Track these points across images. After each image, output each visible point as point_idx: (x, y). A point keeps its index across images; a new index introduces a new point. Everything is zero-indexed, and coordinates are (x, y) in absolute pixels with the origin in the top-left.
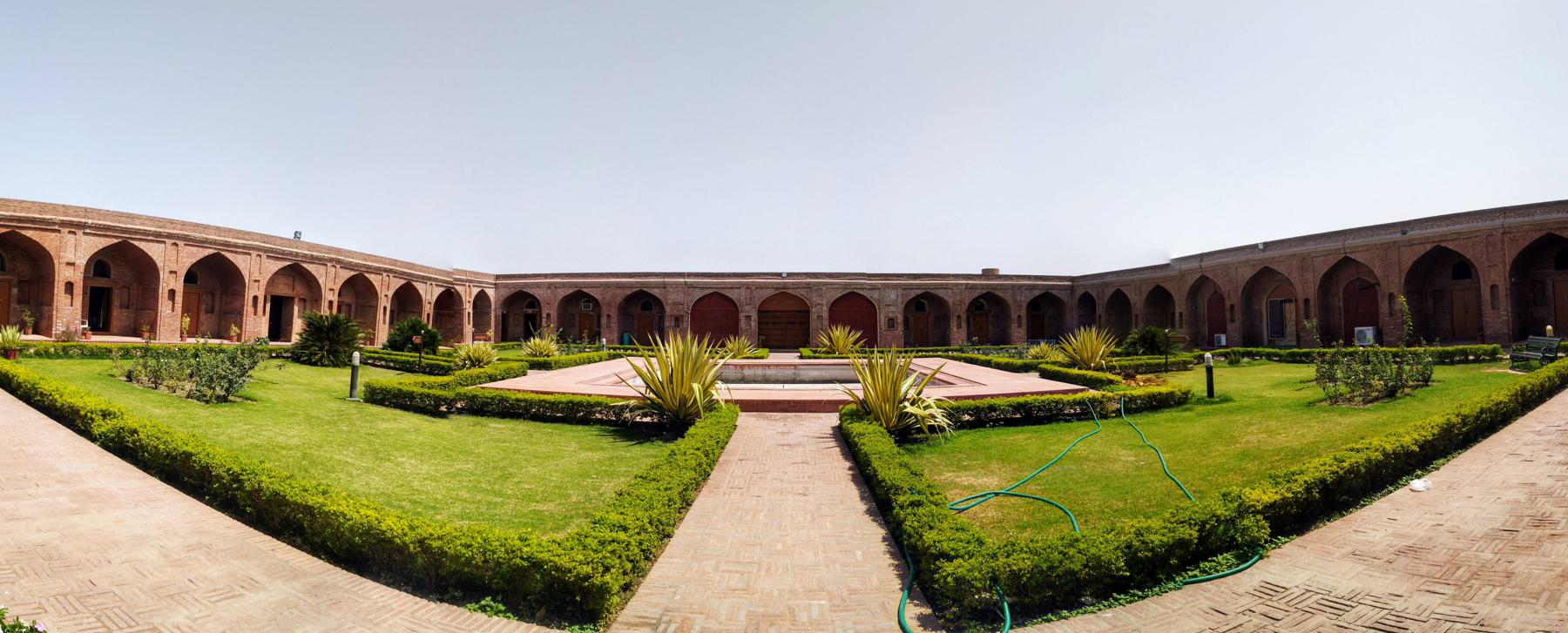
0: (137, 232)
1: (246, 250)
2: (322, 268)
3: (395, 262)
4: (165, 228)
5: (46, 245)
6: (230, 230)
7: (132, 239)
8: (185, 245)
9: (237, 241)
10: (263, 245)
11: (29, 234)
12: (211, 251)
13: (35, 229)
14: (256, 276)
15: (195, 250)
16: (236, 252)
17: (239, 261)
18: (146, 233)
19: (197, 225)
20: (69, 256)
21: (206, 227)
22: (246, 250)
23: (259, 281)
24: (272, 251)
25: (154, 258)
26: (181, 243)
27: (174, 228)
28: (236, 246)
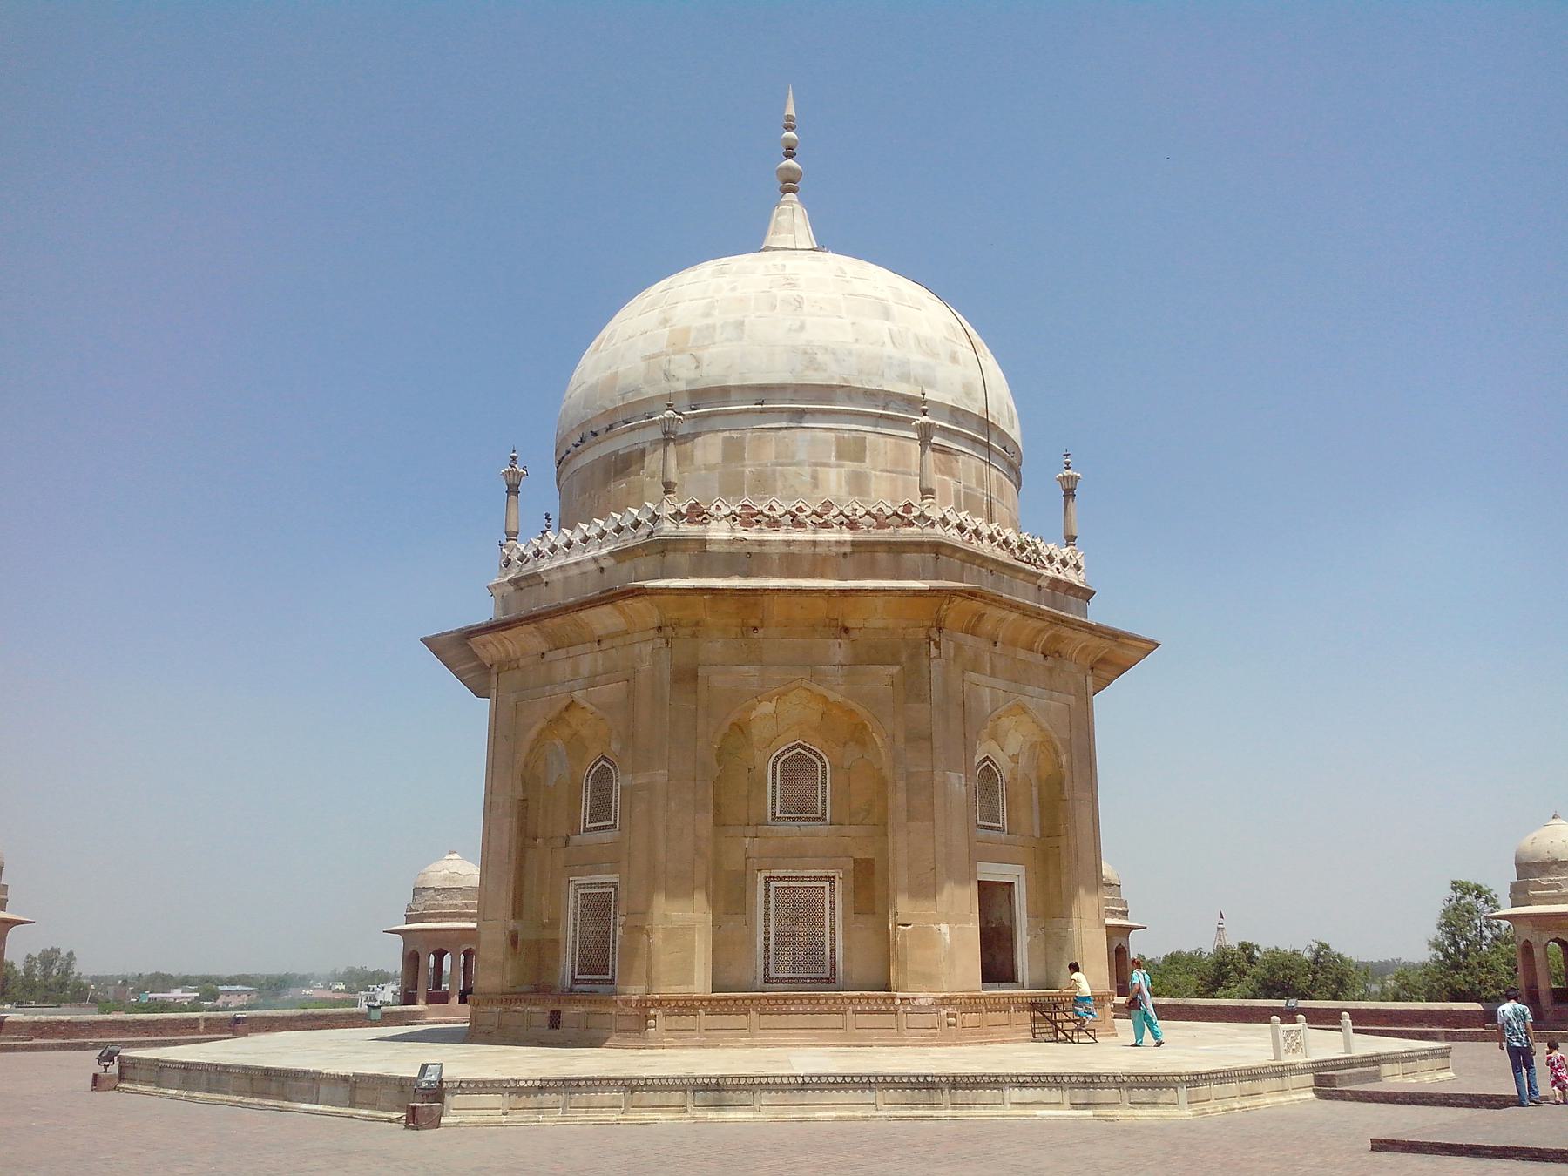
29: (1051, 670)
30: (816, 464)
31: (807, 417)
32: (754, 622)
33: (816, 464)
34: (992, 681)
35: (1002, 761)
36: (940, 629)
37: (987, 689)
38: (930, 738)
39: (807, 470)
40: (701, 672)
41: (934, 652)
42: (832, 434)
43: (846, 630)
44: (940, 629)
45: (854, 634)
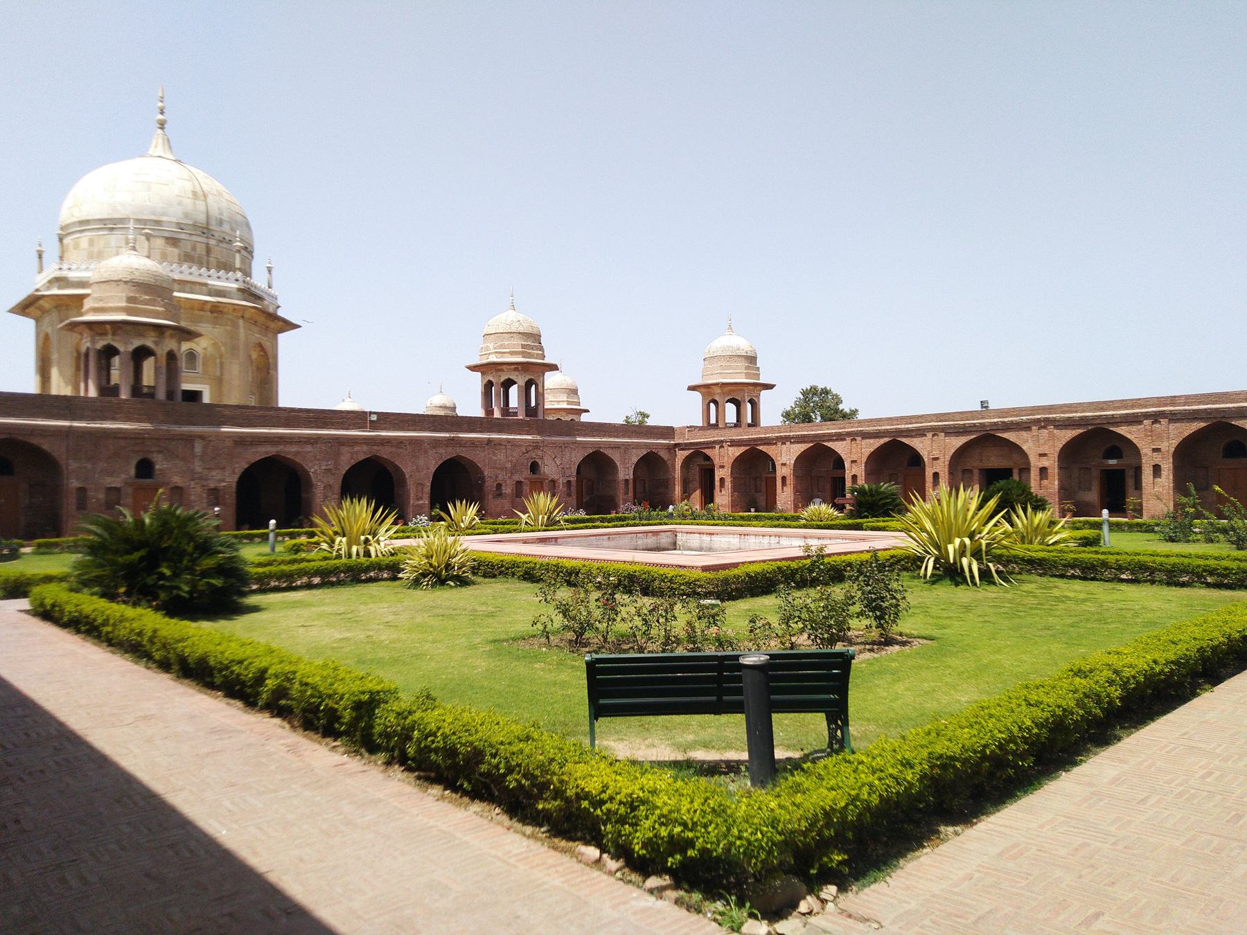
0: (824, 435)
1: (920, 433)
2: (1024, 434)
3: (1173, 400)
4: (845, 428)
5: (770, 454)
6: (902, 418)
7: (823, 441)
8: (863, 438)
9: (907, 426)
10: (940, 423)
11: (761, 448)
12: (887, 440)
13: (764, 444)
14: (936, 454)
15: (872, 441)
16: (912, 436)
17: (916, 443)
18: (830, 435)
19: (871, 420)
20: (784, 460)
21: (879, 420)
22: (920, 433)
23: (937, 459)
24: (949, 427)
25: (839, 452)
26: (859, 439)
27: (852, 427)
28: (908, 430)
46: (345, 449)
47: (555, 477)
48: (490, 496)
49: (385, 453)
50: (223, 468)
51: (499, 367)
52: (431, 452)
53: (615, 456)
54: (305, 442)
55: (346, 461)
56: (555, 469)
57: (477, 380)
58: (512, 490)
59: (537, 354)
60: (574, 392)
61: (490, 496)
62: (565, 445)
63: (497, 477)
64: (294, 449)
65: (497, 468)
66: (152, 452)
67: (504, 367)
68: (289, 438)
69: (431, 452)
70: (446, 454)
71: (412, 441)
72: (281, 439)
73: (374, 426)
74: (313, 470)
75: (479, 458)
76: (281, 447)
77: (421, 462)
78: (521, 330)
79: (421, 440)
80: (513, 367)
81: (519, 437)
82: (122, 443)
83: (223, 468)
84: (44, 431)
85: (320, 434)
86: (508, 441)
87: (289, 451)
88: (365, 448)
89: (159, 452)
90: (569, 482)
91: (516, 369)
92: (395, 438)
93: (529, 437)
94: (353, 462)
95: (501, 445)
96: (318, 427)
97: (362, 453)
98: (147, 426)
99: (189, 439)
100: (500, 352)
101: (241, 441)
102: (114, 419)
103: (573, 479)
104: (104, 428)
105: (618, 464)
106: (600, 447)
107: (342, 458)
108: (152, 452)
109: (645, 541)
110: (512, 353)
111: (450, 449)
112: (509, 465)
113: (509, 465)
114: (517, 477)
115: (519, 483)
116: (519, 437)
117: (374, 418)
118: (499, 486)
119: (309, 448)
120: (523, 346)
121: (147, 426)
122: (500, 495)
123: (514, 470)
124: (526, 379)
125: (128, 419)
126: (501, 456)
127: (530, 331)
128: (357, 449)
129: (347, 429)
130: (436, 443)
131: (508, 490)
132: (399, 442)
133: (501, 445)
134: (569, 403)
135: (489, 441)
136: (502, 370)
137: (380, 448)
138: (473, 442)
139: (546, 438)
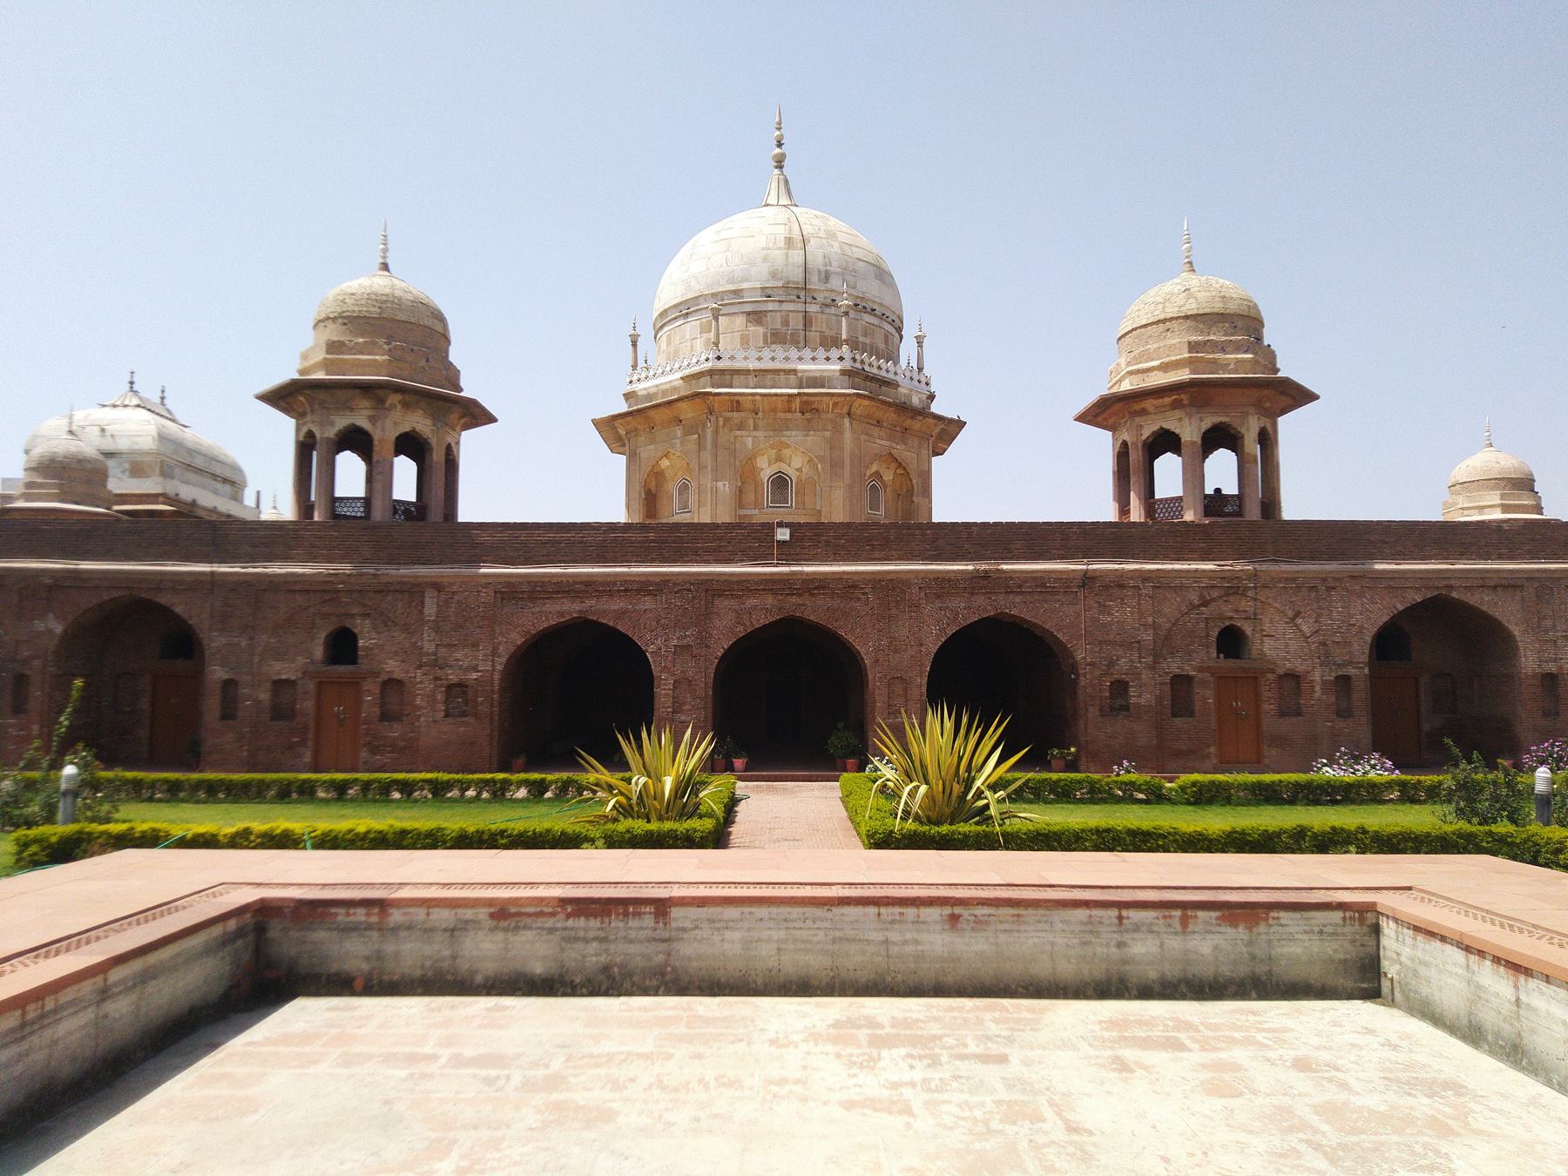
29: (809, 420)
30: (693, 339)
31: (689, 316)
32: (653, 425)
33: (693, 339)
34: (754, 433)
35: (791, 472)
36: (711, 414)
37: (750, 439)
38: (706, 468)
39: (689, 343)
40: (638, 452)
41: (709, 424)
42: (698, 322)
43: (681, 421)
44: (711, 414)
45: (683, 422)
46: (723, 604)
47: (1300, 667)
48: (1093, 712)
49: (814, 610)
50: (475, 645)
51: (1137, 407)
52: (927, 609)
53: (1508, 613)
54: (638, 591)
55: (725, 630)
56: (1294, 646)
57: (1101, 445)
58: (1159, 699)
59: (1238, 361)
60: (1525, 484)
61: (1093, 712)
62: (1329, 584)
63: (1111, 664)
64: (616, 604)
65: (1112, 643)
66: (353, 616)
67: (1149, 404)
68: (602, 584)
69: (927, 609)
70: (969, 611)
71: (876, 581)
72: (589, 587)
73: (788, 552)
74: (652, 648)
75: (1054, 618)
76: (590, 603)
77: (902, 630)
78: (1191, 307)
79: (901, 581)
80: (1167, 400)
81: (1177, 566)
82: (300, 599)
83: (475, 645)
84: (177, 580)
85: (666, 574)
86: (1146, 577)
87: (606, 610)
88: (770, 600)
89: (366, 615)
90: (1344, 682)
91: (1176, 405)
92: (840, 577)
93: (1209, 566)
94: (741, 631)
95: (1121, 586)
96: (665, 560)
97: (762, 612)
98: (345, 568)
99: (414, 591)
100: (1138, 372)
101: (510, 592)
102: (287, 558)
103: (1359, 672)
104: (267, 575)
105: (1516, 631)
106: (1451, 587)
107: (717, 622)
108: (353, 616)
109: (1174, 944)
110: (1165, 367)
111: (980, 600)
112: (1148, 637)
113: (1148, 637)
114: (1174, 666)
115: (1181, 683)
116: (1177, 566)
117: (783, 534)
118: (1120, 688)
119: (648, 603)
120: (1193, 347)
121: (345, 568)
122: (1126, 708)
123: (1164, 645)
124: (1208, 422)
125: (312, 558)
126: (1123, 614)
127: (1218, 307)
128: (750, 602)
129: (728, 561)
130: (944, 584)
131: (1141, 697)
132: (849, 585)
133: (1121, 586)
134: (1506, 508)
135: (1088, 579)
136: (1143, 412)
137: (806, 599)
138: (1039, 580)
139: (1264, 567)
